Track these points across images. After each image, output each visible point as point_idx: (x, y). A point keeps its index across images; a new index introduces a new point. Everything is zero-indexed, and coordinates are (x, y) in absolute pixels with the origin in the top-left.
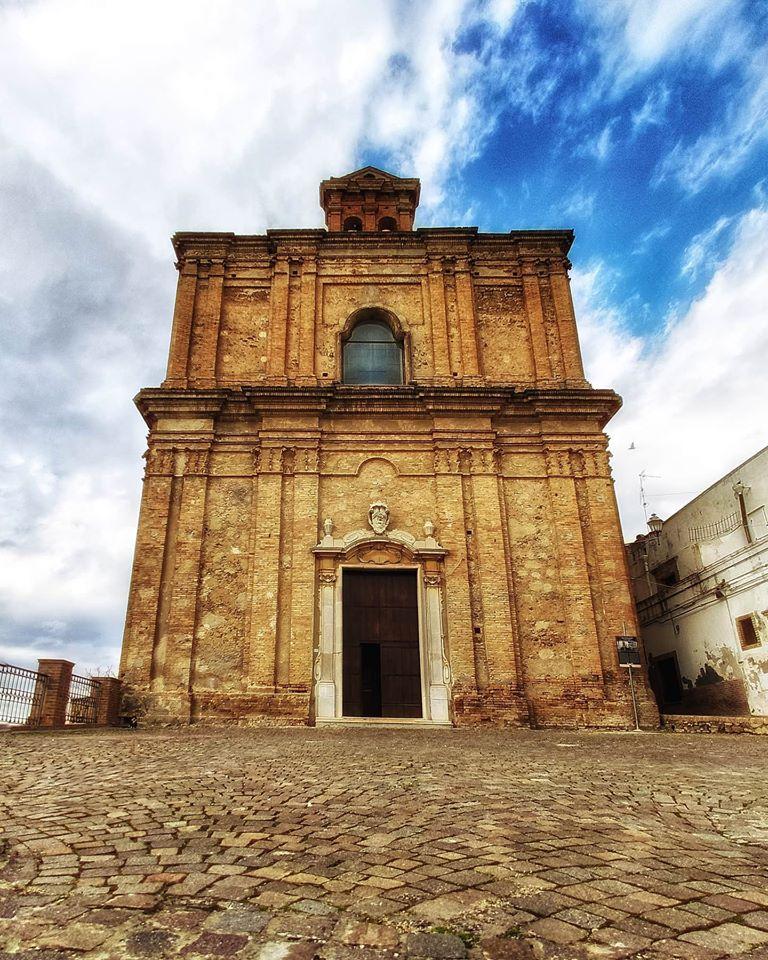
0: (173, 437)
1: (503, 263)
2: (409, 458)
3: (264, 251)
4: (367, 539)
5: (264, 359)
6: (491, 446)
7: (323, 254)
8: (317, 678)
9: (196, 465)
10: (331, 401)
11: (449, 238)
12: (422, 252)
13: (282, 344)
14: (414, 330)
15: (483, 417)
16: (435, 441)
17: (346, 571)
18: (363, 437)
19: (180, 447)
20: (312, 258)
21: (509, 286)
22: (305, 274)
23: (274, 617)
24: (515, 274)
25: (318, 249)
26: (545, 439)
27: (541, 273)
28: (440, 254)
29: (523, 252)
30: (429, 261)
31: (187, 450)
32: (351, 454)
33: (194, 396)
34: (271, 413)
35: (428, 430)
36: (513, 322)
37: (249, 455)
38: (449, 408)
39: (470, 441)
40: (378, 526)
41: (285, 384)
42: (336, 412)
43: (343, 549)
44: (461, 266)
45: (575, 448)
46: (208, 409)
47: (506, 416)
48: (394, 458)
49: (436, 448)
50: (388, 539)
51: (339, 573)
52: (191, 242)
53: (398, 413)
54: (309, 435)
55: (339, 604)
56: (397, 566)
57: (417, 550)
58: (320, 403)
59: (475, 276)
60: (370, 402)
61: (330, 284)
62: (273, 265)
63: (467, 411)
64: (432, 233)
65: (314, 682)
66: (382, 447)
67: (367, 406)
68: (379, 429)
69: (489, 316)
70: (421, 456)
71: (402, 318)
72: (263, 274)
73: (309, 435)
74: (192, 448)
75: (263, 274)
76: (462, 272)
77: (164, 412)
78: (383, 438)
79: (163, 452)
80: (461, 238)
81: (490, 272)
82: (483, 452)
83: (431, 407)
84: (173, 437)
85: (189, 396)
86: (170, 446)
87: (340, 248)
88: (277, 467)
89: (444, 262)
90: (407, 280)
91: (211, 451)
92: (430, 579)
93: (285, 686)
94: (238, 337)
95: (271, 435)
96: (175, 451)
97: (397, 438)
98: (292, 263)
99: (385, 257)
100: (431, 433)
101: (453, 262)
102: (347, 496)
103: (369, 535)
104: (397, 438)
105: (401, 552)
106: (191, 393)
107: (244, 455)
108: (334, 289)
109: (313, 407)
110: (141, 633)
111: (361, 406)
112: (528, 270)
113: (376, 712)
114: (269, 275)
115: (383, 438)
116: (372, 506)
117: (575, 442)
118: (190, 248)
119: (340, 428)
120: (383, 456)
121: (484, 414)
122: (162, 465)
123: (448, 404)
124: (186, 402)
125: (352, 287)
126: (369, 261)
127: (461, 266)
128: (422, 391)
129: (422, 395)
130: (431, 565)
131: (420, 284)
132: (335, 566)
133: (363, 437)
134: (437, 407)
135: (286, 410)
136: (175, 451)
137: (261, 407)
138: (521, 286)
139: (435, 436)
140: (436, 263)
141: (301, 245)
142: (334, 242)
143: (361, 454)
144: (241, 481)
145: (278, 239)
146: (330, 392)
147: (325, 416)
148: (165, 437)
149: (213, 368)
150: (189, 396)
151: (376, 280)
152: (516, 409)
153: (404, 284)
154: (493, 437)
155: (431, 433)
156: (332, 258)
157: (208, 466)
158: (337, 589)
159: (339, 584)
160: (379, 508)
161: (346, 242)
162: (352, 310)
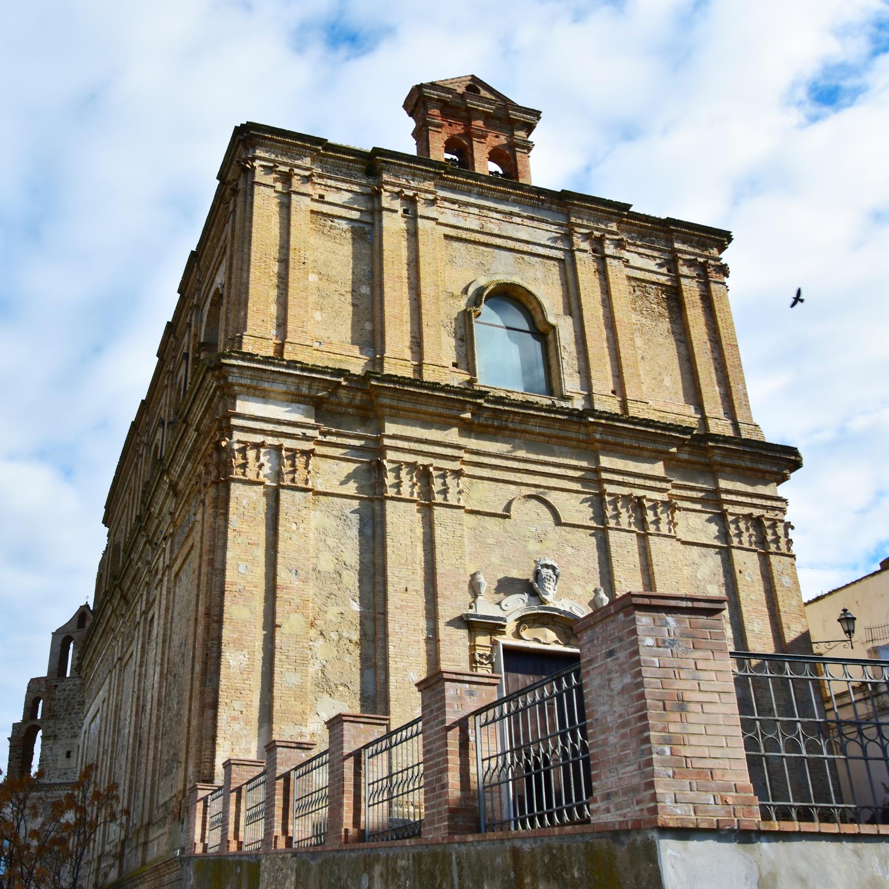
1: (656, 254)
11: (597, 210)
33: (298, 373)
52: (266, 138)
53: (557, 437)
64: (578, 200)
67: (521, 422)
69: (644, 320)
77: (249, 387)
85: (291, 371)
94: (334, 287)
99: (519, 216)
102: (499, 544)
106: (295, 368)
108: (456, 245)
118: (262, 145)
124: (283, 378)
150: (291, 371)
151: (510, 244)
156: (453, 202)
161: (471, 184)
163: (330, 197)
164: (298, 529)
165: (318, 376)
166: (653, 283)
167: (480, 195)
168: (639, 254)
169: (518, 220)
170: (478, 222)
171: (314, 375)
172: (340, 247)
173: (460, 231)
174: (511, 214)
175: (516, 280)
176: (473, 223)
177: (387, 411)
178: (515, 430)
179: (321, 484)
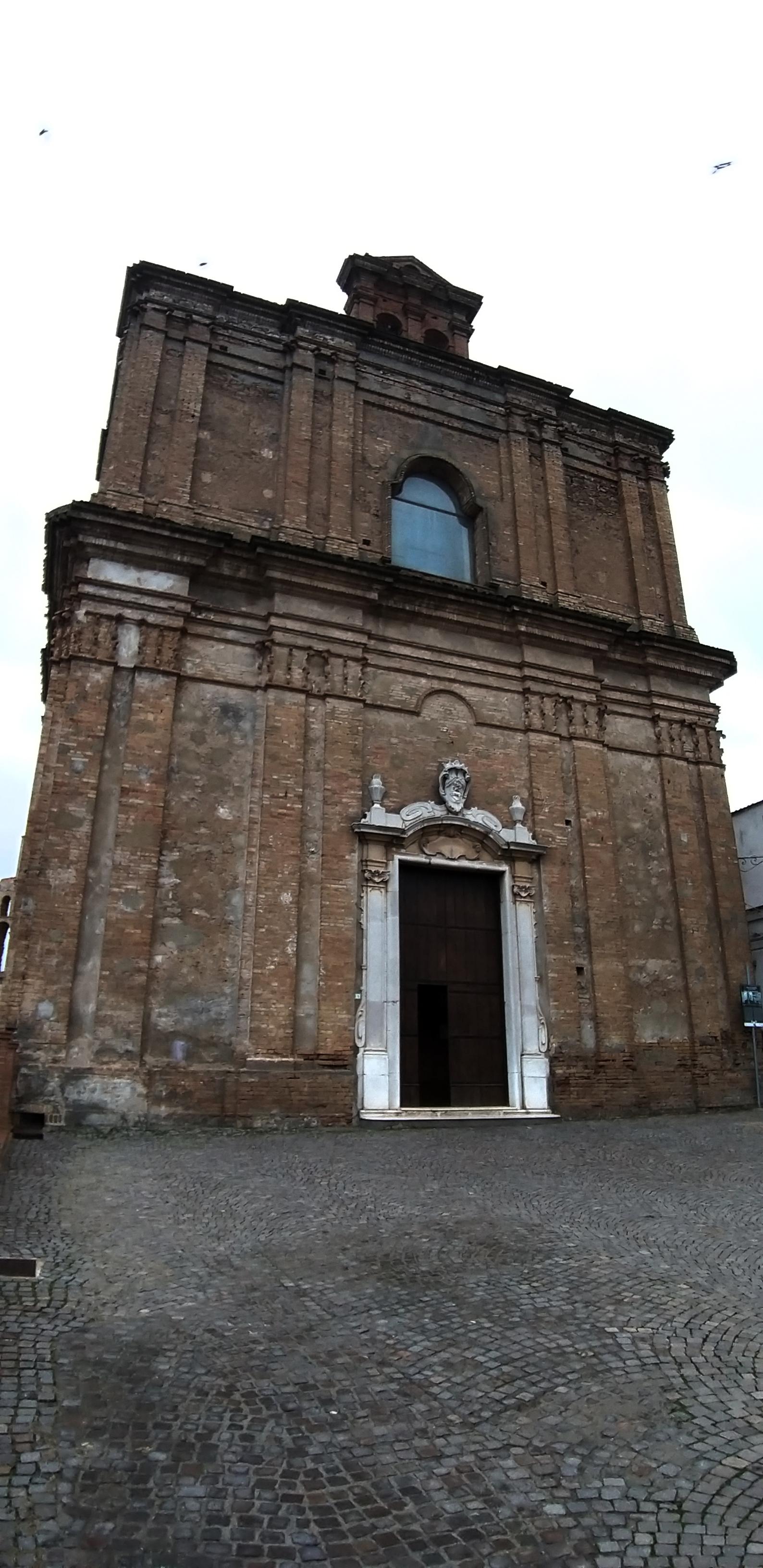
0: (117, 595)
1: (596, 446)
2: (490, 697)
3: (272, 325)
4: (438, 818)
5: (268, 493)
6: (593, 698)
7: (365, 357)
8: (360, 1044)
9: (159, 652)
10: (389, 591)
12: (499, 398)
13: (303, 478)
14: (490, 505)
15: (585, 656)
16: (524, 678)
17: (403, 864)
18: (427, 655)
19: (128, 613)
20: (351, 358)
21: (602, 478)
22: (341, 379)
23: (292, 938)
24: (609, 464)
25: (357, 348)
26: (656, 701)
27: (639, 473)
28: (524, 409)
29: (619, 438)
30: (508, 415)
31: (141, 623)
32: (410, 677)
33: (166, 533)
34: (291, 590)
35: (516, 659)
36: (607, 527)
37: (247, 650)
38: (546, 634)
39: (568, 687)
40: (455, 800)
41: (310, 545)
42: (388, 607)
43: (403, 831)
44: (549, 433)
45: (688, 718)
46: (185, 559)
47: (610, 660)
48: (468, 692)
49: (526, 692)
50: (467, 821)
51: (394, 869)
53: (478, 627)
54: (349, 636)
55: (394, 920)
56: (477, 865)
57: (508, 844)
58: (370, 589)
59: (565, 452)
60: (441, 603)
61: (373, 405)
62: (289, 349)
63: (567, 643)
65: (356, 1049)
66: (452, 674)
68: (447, 645)
69: (580, 512)
70: (505, 697)
71: (475, 485)
72: (270, 358)
73: (349, 636)
74: (151, 618)
75: (270, 358)
76: (553, 443)
77: (106, 548)
78: (455, 660)
79: (98, 618)
80: (551, 397)
81: (581, 453)
82: (585, 704)
83: (523, 629)
84: (117, 595)
85: (158, 531)
86: (113, 610)
87: (389, 357)
88: (297, 675)
89: (528, 421)
90: (479, 430)
91: (184, 632)
92: (520, 888)
93: (307, 1057)
95: (290, 624)
96: (120, 620)
97: (474, 664)
98: (319, 357)
99: (452, 390)
100: (520, 666)
101: (539, 424)
103: (439, 811)
104: (474, 664)
105: (482, 842)
106: (163, 527)
107: (239, 649)
108: (376, 412)
109: (359, 593)
110: (50, 952)
111: (428, 608)
112: (626, 464)
113: (445, 1101)
114: (281, 364)
115: (455, 660)
116: (448, 766)
117: (685, 711)
119: (392, 632)
120: (456, 687)
121: (587, 652)
122: (96, 643)
123: (547, 628)
125: (402, 417)
126: (429, 388)
127: (549, 433)
128: (517, 605)
129: (516, 608)
130: (522, 868)
131: (497, 441)
132: (389, 858)
133: (427, 655)
134: (530, 630)
135: (316, 589)
136: (120, 620)
137: (277, 575)
138: (616, 482)
139: (527, 672)
140: (518, 419)
141: (333, 334)
142: (382, 346)
143: (423, 681)
144: (233, 692)
145: (300, 316)
146: (390, 575)
147: (373, 610)
148: (104, 592)
149: (188, 490)
150: (158, 531)
151: (440, 418)
152: (623, 653)
153: (475, 434)
154: (597, 686)
155: (520, 666)
156: (378, 367)
157: (178, 659)
158: (389, 894)
159: (394, 885)
160: (456, 770)
162: (405, 454)
163: (232, 349)
164: (155, 719)
165: (193, 539)
166: (592, 475)
167: (409, 363)
168: (579, 444)
169: (450, 394)
170: (404, 391)
171: (187, 538)
172: (241, 405)
173: (382, 398)
174: (442, 386)
175: (443, 456)
176: (398, 392)
177: (279, 585)
178: (430, 617)
179: (191, 669)
